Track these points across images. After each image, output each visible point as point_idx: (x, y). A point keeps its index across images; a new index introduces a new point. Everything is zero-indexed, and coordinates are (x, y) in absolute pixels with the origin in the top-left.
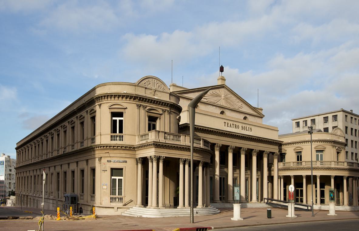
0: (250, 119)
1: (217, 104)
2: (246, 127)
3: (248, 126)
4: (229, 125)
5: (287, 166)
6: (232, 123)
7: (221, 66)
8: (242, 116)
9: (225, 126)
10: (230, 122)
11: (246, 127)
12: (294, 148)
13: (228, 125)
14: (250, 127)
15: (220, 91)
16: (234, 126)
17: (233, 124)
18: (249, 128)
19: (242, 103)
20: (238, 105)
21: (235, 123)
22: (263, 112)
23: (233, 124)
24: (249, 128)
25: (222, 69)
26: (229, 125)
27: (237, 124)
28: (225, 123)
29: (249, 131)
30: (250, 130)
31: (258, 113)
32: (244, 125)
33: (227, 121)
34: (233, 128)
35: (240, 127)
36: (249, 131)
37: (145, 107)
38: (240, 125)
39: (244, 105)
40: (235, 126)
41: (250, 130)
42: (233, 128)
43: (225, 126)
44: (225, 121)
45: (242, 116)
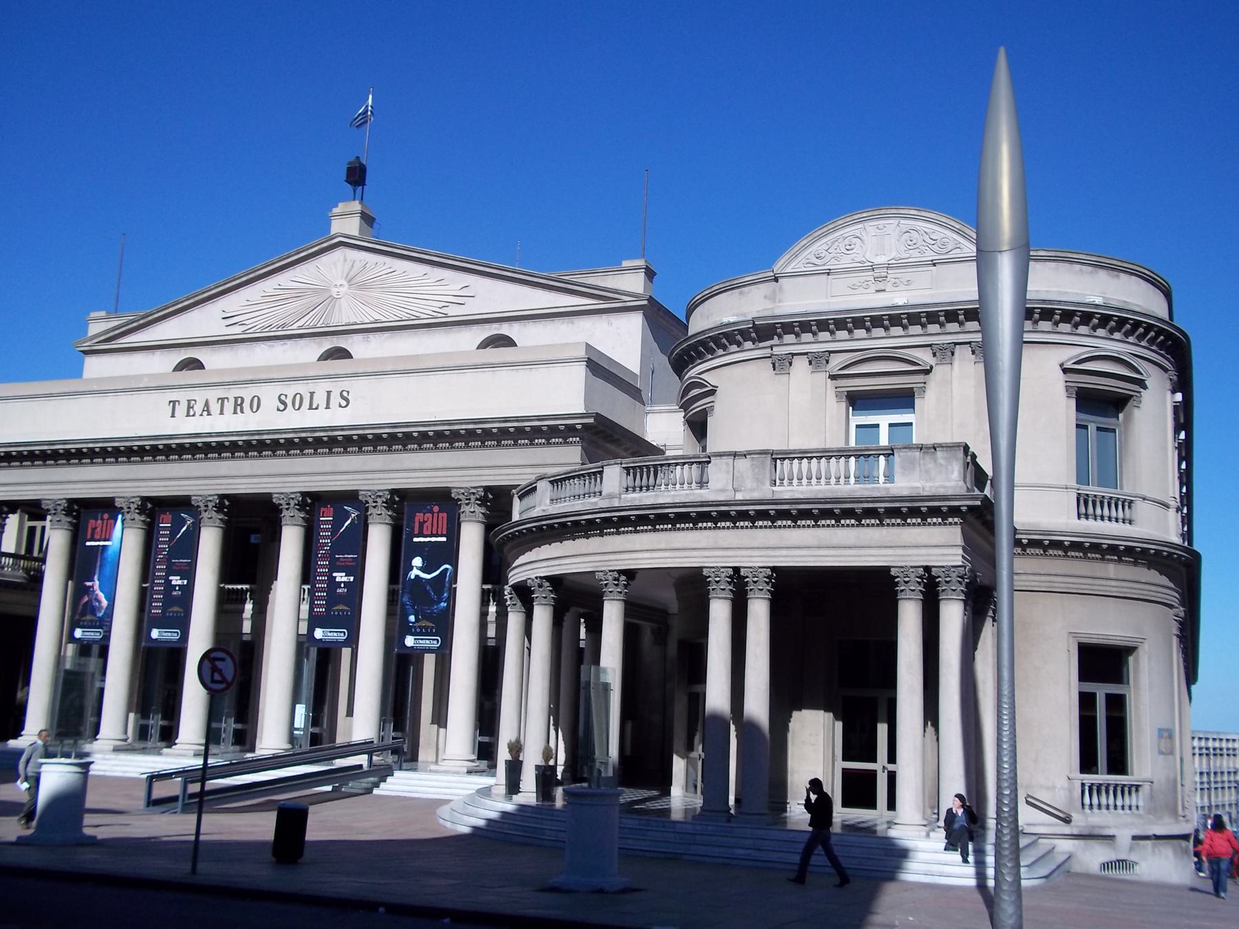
1: (300, 328)
2: (312, 394)
4: (198, 408)
6: (213, 395)
7: (353, 159)
9: (173, 416)
10: (200, 396)
11: (312, 394)
13: (189, 407)
14: (336, 387)
16: (229, 406)
18: (329, 393)
24: (329, 393)
26: (198, 408)
27: (247, 393)
29: (328, 407)
30: (336, 399)
32: (290, 390)
33: (182, 396)
34: (222, 413)
36: (328, 407)
38: (268, 395)
40: (236, 404)
41: (336, 399)
42: (222, 413)
43: (173, 416)
44: (174, 395)
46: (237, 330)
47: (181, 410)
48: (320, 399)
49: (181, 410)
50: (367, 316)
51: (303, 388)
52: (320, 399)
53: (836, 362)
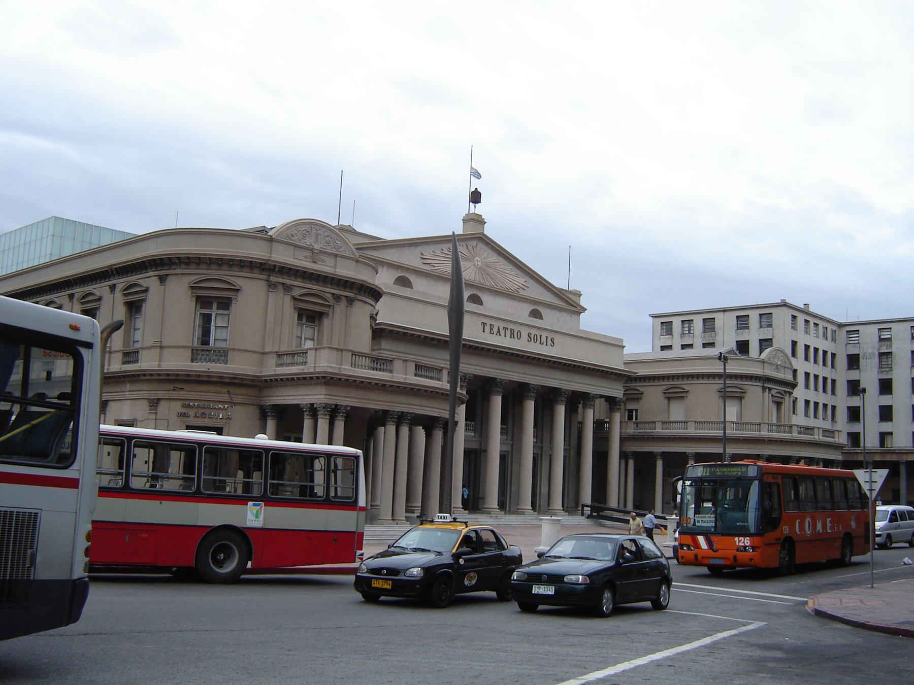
0: (551, 320)
3: (544, 334)
4: (495, 330)
5: (643, 431)
6: (502, 325)
8: (529, 308)
10: (496, 324)
12: (665, 387)
13: (491, 329)
15: (470, 248)
17: (505, 329)
19: (527, 279)
20: (516, 281)
21: (510, 326)
22: (583, 302)
23: (505, 329)
25: (476, 197)
26: (495, 330)
28: (484, 324)
31: (569, 303)
32: (533, 332)
33: (488, 322)
35: (524, 336)
37: (287, 288)
39: (531, 283)
41: (549, 342)
45: (529, 308)
46: (428, 268)
47: (487, 329)
48: (544, 339)
49: (487, 329)
50: (489, 283)
51: (538, 333)
52: (544, 339)
53: (773, 392)
